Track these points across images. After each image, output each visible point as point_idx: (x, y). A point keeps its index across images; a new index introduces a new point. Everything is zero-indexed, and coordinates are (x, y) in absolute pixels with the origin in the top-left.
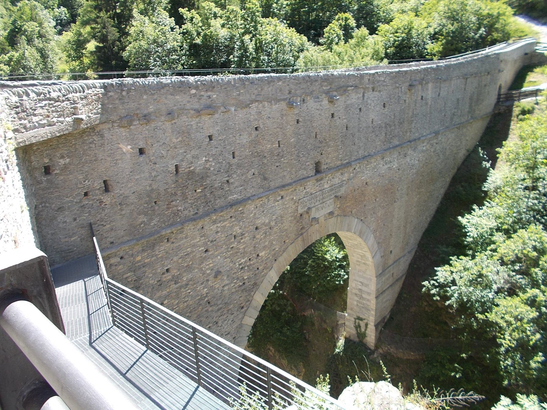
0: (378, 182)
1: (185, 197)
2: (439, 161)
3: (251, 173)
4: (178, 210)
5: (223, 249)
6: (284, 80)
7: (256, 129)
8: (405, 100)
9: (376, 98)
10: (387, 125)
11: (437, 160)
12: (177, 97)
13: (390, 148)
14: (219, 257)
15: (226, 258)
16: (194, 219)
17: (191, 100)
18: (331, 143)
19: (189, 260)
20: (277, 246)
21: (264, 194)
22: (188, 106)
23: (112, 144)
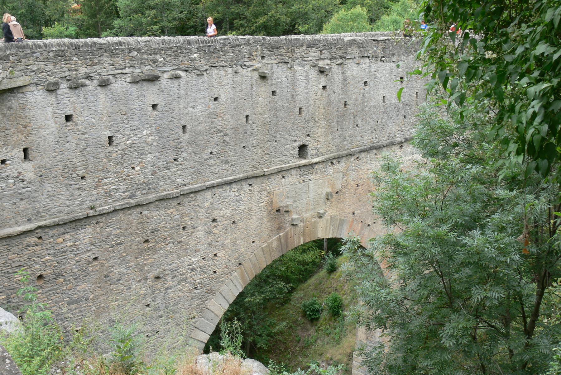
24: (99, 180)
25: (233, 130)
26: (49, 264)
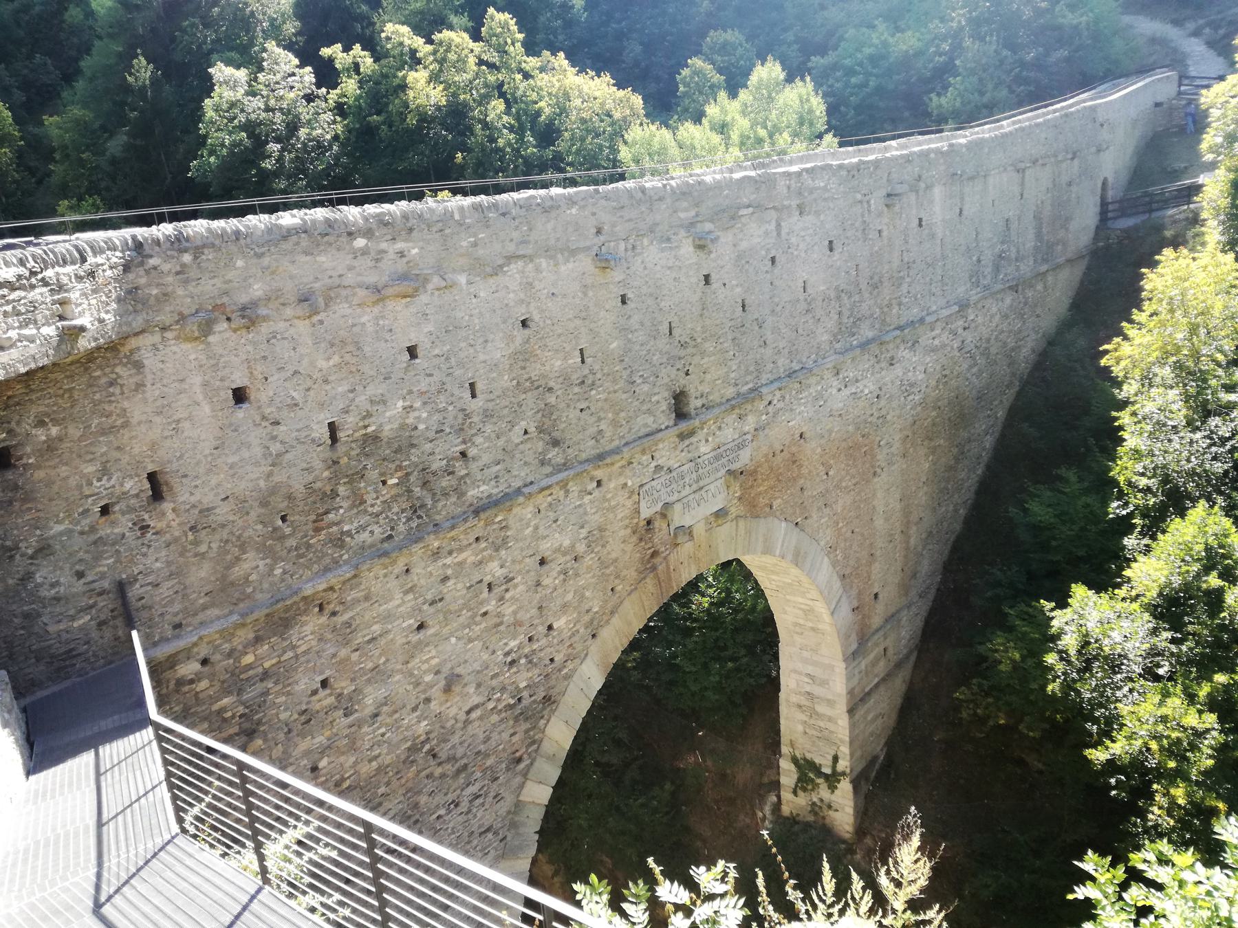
0: (830, 431)
1: (359, 501)
2: (975, 370)
3: (518, 430)
4: (342, 533)
5: (461, 619)
6: (582, 203)
7: (524, 323)
8: (880, 232)
9: (811, 231)
10: (840, 292)
11: (971, 367)
12: (322, 259)
13: (852, 348)
14: (453, 640)
15: (470, 640)
16: (383, 551)
17: (356, 263)
18: (709, 346)
19: (377, 653)
20: (596, 602)
21: (554, 479)
22: (350, 279)
23: (165, 381)
24: (318, 515)
25: (561, 380)
26: (229, 714)
